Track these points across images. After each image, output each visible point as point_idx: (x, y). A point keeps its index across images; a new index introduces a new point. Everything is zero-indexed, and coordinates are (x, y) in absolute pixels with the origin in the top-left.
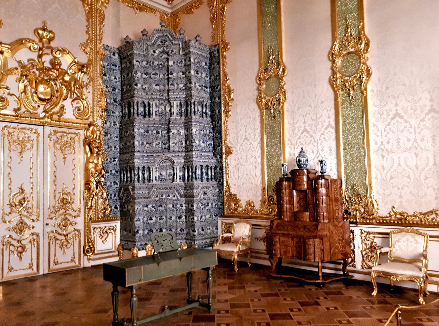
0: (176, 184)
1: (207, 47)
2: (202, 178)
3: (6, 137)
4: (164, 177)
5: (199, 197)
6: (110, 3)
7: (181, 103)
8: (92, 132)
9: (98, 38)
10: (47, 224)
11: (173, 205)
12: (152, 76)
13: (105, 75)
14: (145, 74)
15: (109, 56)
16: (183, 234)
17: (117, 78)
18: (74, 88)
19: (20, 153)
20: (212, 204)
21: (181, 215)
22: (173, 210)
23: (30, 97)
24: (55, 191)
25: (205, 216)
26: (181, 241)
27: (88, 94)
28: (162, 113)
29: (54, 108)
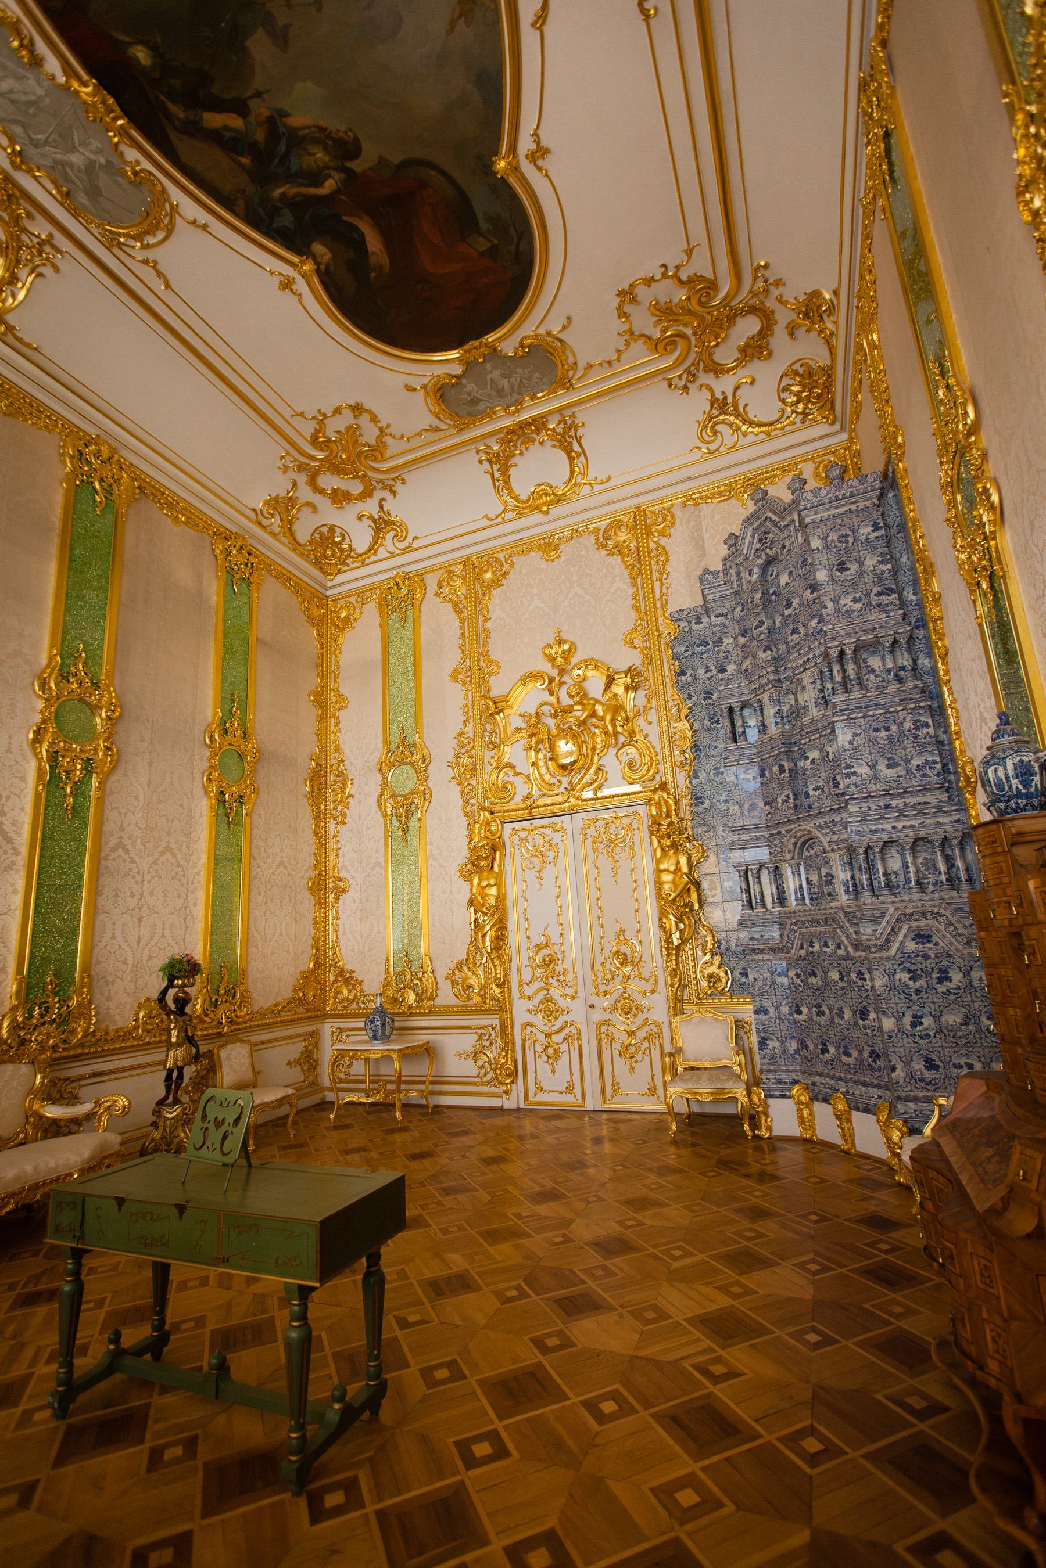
0: (837, 908)
1: (870, 479)
2: (908, 881)
3: (517, 847)
4: (816, 890)
5: (893, 951)
6: (677, 523)
7: (821, 673)
8: (659, 804)
9: (659, 605)
10: (592, 1006)
11: (841, 973)
12: (755, 632)
13: (682, 673)
14: (743, 635)
15: (686, 629)
16: (879, 1070)
17: (713, 668)
18: (621, 727)
19: (539, 871)
20: (967, 973)
21: (865, 1007)
22: (842, 988)
23: (543, 771)
24: (602, 938)
25: (937, 1018)
26: (880, 1092)
27: (650, 729)
28: (792, 713)
29: (585, 775)
